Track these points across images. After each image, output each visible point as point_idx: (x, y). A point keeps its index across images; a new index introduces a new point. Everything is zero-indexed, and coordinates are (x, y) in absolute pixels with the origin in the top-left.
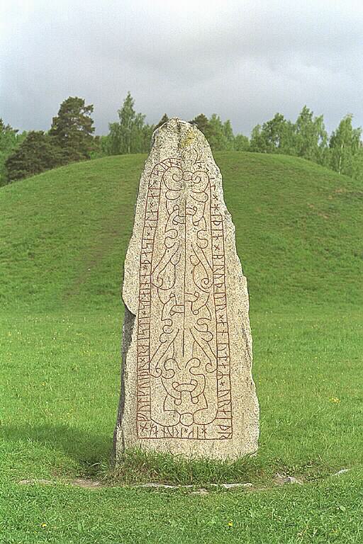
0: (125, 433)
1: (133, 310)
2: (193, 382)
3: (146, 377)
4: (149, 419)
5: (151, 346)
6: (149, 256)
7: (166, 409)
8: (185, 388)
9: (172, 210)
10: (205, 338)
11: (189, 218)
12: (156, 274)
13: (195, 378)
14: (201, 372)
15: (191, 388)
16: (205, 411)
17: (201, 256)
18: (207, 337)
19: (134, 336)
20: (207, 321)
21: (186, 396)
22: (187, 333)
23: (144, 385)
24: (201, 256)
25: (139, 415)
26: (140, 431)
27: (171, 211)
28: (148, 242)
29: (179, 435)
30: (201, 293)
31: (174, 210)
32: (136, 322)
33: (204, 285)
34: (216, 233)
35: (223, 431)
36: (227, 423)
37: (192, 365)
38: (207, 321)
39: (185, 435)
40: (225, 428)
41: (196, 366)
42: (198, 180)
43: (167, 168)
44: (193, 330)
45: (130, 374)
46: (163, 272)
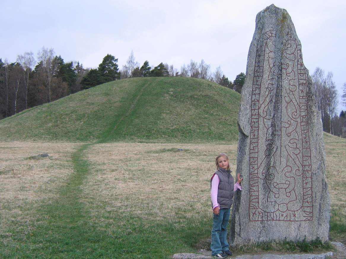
0: (241, 218)
1: (247, 132)
2: (287, 182)
3: (255, 179)
5: (259, 158)
6: (257, 96)
7: (269, 200)
8: (282, 186)
10: (295, 152)
11: (284, 71)
12: (262, 108)
13: (289, 179)
15: (286, 186)
16: (295, 202)
17: (292, 96)
18: (297, 151)
19: (247, 150)
20: (296, 141)
22: (283, 149)
23: (254, 185)
24: (292, 96)
25: (251, 205)
27: (271, 66)
28: (256, 86)
30: (292, 121)
31: (274, 66)
32: (248, 141)
33: (294, 116)
34: (301, 81)
35: (306, 215)
36: (308, 210)
37: (286, 171)
38: (296, 141)
39: (282, 218)
40: (308, 213)
41: (289, 171)
42: (289, 46)
43: (269, 37)
44: (287, 147)
46: (267, 107)
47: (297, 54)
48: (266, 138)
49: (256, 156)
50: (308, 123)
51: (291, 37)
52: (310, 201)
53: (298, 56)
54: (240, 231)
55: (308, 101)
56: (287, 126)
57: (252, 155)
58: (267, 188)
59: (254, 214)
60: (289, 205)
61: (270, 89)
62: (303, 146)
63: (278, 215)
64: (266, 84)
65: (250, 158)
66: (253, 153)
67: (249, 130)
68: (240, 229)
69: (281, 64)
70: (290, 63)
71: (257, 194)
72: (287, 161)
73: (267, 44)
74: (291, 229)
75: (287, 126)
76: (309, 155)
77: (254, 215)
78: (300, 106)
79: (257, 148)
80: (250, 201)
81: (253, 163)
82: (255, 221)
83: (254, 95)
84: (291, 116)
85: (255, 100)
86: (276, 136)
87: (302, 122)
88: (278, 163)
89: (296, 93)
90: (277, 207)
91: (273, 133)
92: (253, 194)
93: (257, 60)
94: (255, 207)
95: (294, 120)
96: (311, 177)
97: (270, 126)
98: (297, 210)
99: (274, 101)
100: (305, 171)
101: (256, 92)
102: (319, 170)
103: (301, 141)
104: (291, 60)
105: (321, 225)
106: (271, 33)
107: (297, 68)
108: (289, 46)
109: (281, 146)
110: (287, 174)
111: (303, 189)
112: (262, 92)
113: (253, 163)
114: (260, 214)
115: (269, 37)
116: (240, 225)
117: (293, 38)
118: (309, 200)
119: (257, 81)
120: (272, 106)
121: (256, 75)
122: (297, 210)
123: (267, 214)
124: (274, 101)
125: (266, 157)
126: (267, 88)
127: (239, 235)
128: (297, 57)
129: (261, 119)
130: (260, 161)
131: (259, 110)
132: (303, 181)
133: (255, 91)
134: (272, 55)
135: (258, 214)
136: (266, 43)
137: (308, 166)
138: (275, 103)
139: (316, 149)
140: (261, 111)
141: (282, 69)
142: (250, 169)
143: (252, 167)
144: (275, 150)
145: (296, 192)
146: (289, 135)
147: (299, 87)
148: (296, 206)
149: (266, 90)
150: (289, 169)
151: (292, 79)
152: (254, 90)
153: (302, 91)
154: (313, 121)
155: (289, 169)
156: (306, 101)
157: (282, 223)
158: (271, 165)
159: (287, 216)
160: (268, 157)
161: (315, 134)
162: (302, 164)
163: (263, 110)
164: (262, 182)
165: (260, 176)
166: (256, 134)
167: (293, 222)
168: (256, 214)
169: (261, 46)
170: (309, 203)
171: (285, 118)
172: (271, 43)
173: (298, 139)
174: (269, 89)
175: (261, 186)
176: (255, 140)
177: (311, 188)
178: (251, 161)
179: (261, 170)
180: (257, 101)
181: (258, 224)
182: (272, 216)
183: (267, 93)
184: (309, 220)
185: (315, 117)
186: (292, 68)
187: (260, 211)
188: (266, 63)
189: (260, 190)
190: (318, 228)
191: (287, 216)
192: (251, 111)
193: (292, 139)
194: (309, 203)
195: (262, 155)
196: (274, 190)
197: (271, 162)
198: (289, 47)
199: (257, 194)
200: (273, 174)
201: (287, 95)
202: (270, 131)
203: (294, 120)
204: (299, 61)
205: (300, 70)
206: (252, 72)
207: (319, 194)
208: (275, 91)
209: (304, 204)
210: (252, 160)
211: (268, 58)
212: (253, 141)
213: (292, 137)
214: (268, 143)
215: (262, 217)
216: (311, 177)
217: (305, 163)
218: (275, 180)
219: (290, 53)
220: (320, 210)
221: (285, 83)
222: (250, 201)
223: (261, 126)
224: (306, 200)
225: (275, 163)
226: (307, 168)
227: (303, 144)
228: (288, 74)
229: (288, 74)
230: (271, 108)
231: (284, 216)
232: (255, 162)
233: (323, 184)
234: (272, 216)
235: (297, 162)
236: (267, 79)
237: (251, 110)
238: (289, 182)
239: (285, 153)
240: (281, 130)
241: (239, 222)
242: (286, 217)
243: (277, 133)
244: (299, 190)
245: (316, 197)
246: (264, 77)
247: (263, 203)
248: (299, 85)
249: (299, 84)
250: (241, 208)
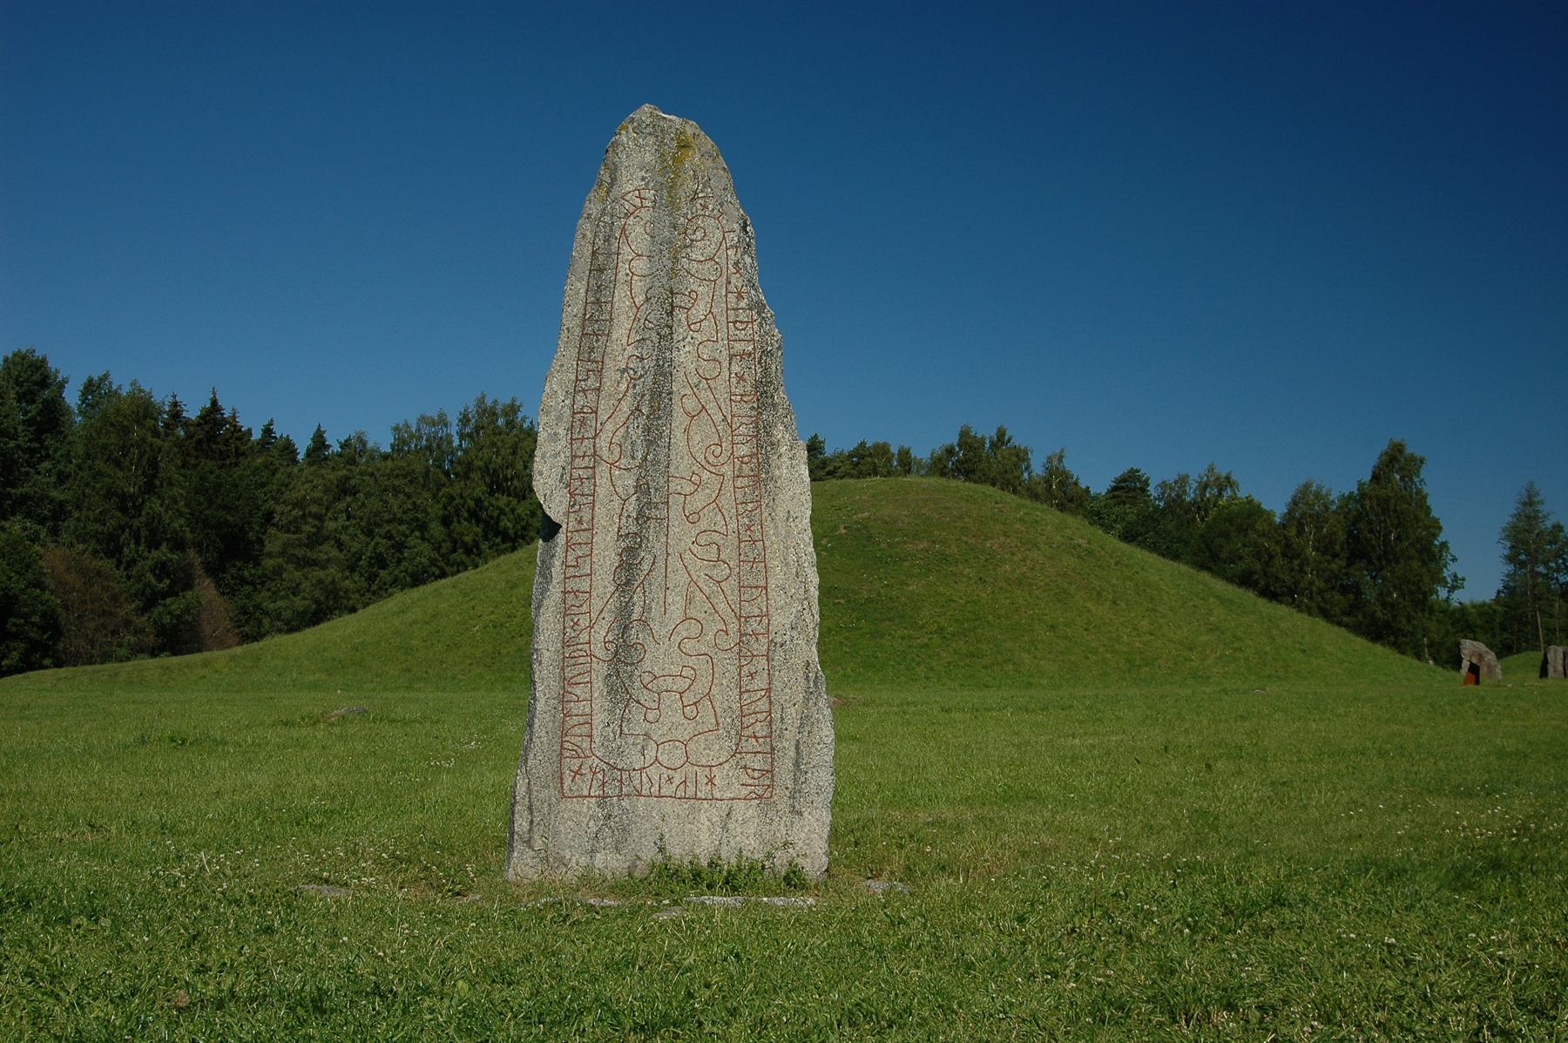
2: (687, 672)
3: (581, 660)
4: (588, 753)
5: (594, 594)
6: (592, 396)
9: (642, 298)
12: (604, 438)
13: (692, 661)
14: (704, 649)
15: (682, 684)
18: (721, 572)
20: (716, 537)
21: (671, 700)
23: (578, 679)
24: (705, 395)
25: (566, 745)
26: (568, 781)
27: (640, 299)
28: (590, 366)
29: (655, 789)
30: (706, 475)
31: (647, 299)
34: (739, 347)
35: (750, 782)
36: (757, 763)
38: (716, 537)
40: (756, 774)
43: (632, 209)
44: (687, 556)
45: (546, 654)
47: (724, 261)
48: (620, 528)
49: (585, 586)
50: (757, 482)
51: (705, 207)
52: (764, 733)
53: (730, 266)
54: (530, 830)
55: (759, 409)
56: (688, 489)
57: (571, 585)
58: (620, 690)
59: (576, 773)
60: (691, 746)
61: (636, 372)
62: (740, 554)
63: (657, 778)
64: (620, 358)
65: (564, 592)
66: (575, 576)
67: (565, 505)
68: (532, 822)
69: (672, 293)
70: (700, 289)
71: (587, 710)
72: (689, 601)
73: (627, 232)
74: (699, 825)
75: (688, 489)
76: (762, 583)
77: (578, 776)
78: (731, 427)
79: (588, 562)
80: (564, 733)
81: (575, 610)
82: (579, 796)
83: (581, 394)
84: (701, 458)
85: (585, 410)
86: (652, 523)
87: (738, 477)
88: (656, 612)
89: (720, 385)
90: (651, 753)
91: (640, 514)
92: (576, 708)
93: (593, 282)
94: (579, 751)
95: (711, 469)
96: (767, 656)
97: (632, 491)
98: (720, 764)
99: (645, 410)
100: (746, 635)
101: (589, 382)
102: (795, 633)
103: (733, 538)
104: (705, 280)
105: (800, 814)
106: (639, 197)
107: (725, 306)
108: (699, 235)
109: (668, 554)
110: (689, 646)
111: (741, 693)
112: (607, 383)
113: (575, 610)
114: (595, 773)
115: (632, 209)
116: (530, 809)
117: (713, 210)
118: (762, 731)
119: (592, 350)
120: (638, 427)
121: (589, 330)
122: (720, 764)
123: (619, 773)
124: (645, 410)
125: (617, 590)
127: (529, 843)
128: (724, 270)
129: (602, 469)
130: (597, 604)
131: (597, 441)
132: (741, 667)
133: (584, 380)
134: (641, 265)
135: (589, 776)
136: (623, 230)
137: (759, 619)
138: (648, 417)
139: (787, 564)
140: (602, 442)
141: (673, 307)
142: (565, 628)
143: (572, 620)
144: (646, 566)
145: (717, 705)
146: (692, 518)
147: (730, 364)
148: (715, 750)
149: (622, 378)
150: (695, 629)
151: (708, 340)
152: (580, 378)
153: (741, 378)
154: (777, 473)
155: (695, 629)
156: (752, 408)
157: (668, 806)
158: (635, 616)
159: (685, 781)
160: (623, 591)
161: (782, 514)
162: (737, 611)
164: (601, 669)
165: (598, 650)
166: (586, 516)
167: (705, 802)
168: (581, 775)
169: (607, 240)
170: (761, 740)
171: (681, 464)
172: (639, 229)
173: (723, 530)
174: (632, 372)
175: (599, 684)
176: (582, 537)
177: (769, 690)
178: (569, 603)
179: (601, 632)
180: (590, 413)
181: (589, 808)
182: (636, 782)
183: (623, 387)
184: (760, 797)
185: (785, 459)
186: (709, 306)
187: (595, 765)
188: (621, 293)
189: (596, 695)
190: (792, 823)
191: (685, 781)
192: (571, 444)
193: (705, 531)
194: (761, 740)
195: (603, 584)
196: (644, 697)
197: (634, 605)
198: (699, 238)
199: (587, 710)
200: (640, 644)
201: (688, 391)
202: (632, 507)
203: (711, 469)
204: (733, 281)
205: (733, 309)
206: (577, 321)
207: (792, 712)
208: (650, 379)
209: (743, 743)
210: (570, 599)
211: (627, 275)
212: (577, 538)
213: (703, 525)
214: (623, 545)
215: (604, 784)
216: (767, 656)
217: (747, 609)
218: (646, 665)
219: (703, 259)
220: (797, 764)
221: (684, 356)
222: (564, 733)
223: (601, 491)
224: (749, 732)
225: (646, 608)
226: (754, 625)
227: (742, 545)
228: (693, 324)
229: (693, 324)
230: (637, 434)
231: (677, 781)
232: (582, 606)
233: (808, 676)
234: (636, 782)
235: (722, 606)
236: (624, 341)
237: (571, 439)
238: (692, 672)
239: (679, 578)
240: (668, 502)
241: (527, 799)
242: (682, 786)
243: (654, 512)
244: (726, 697)
245: (782, 719)
246: (614, 336)
247: (606, 738)
248: (731, 359)
249: (731, 357)
250: (535, 755)
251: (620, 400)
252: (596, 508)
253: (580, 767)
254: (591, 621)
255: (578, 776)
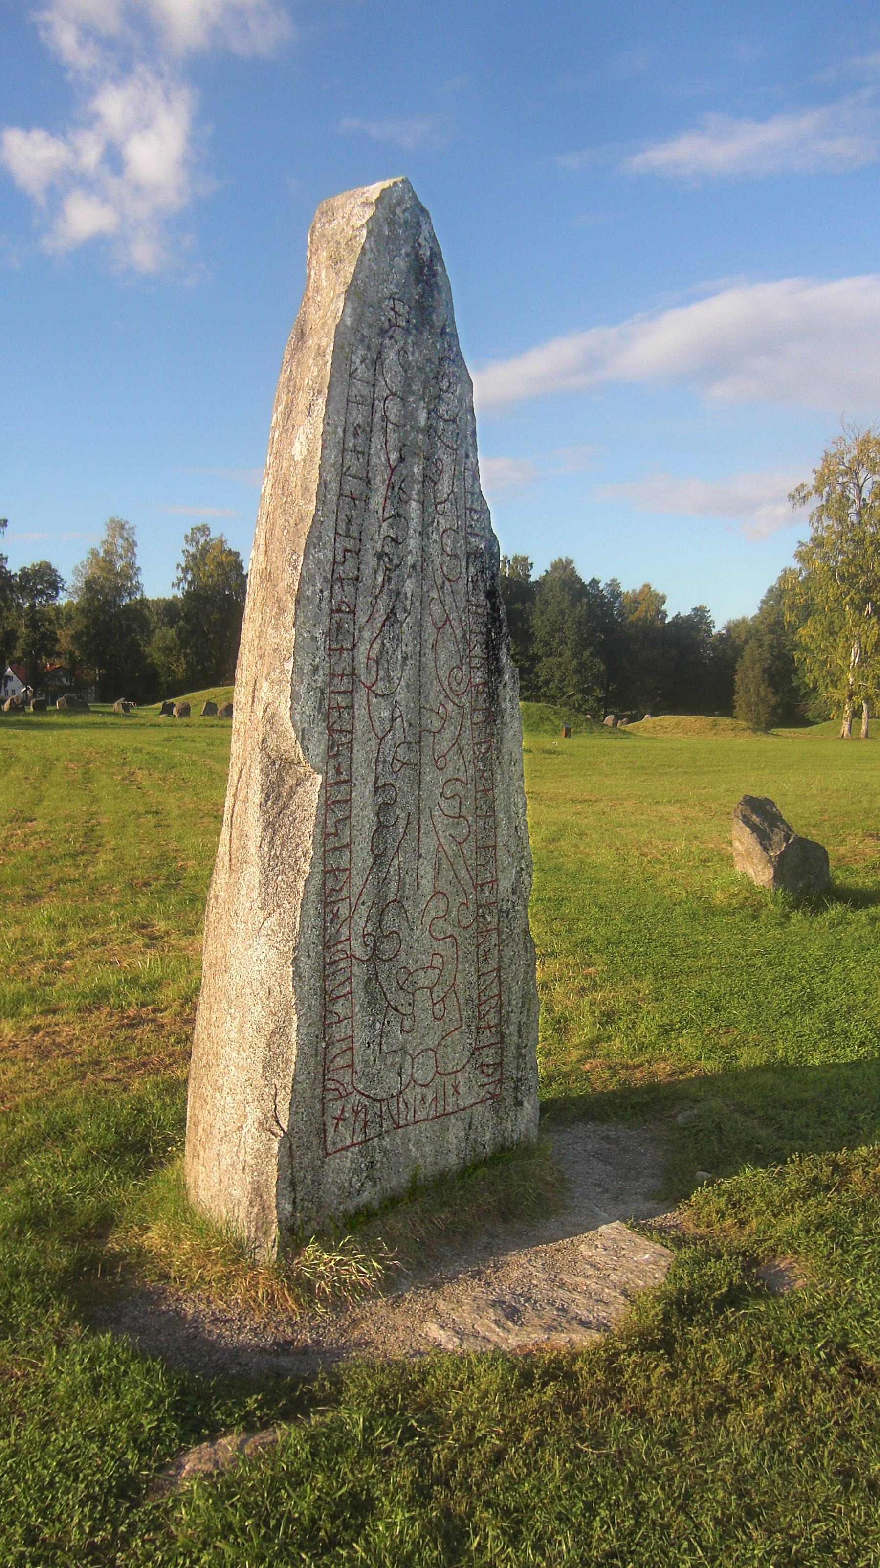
77: (341, 1123)
94: (341, 1088)
126: (380, 556)
129: (360, 698)
143: (332, 911)
163: (366, 655)
175: (360, 996)
179: (360, 923)
232: (341, 889)
251: (376, 597)
252: (355, 751)
253: (343, 1111)
254: (351, 909)
255: (341, 1123)
